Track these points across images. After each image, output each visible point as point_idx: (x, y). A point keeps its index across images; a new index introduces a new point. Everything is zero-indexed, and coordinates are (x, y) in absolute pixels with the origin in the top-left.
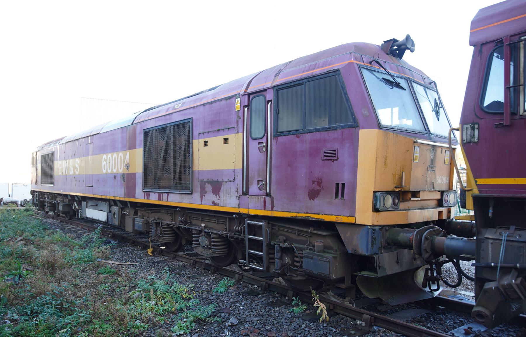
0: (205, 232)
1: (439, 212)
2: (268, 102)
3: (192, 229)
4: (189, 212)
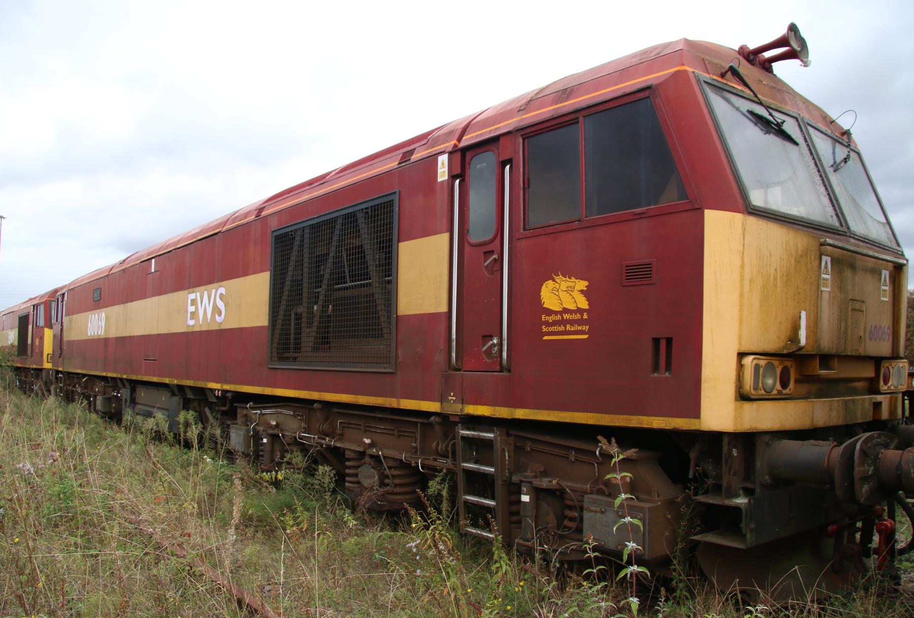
0: (372, 456)
3: (344, 450)
4: (338, 412)
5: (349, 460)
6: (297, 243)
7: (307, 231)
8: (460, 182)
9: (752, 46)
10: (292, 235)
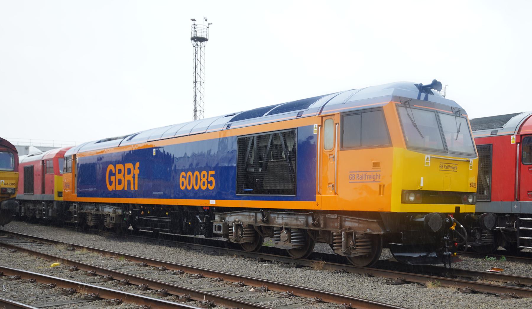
0: (286, 229)
1: (456, 207)
2: (336, 124)
3: (273, 227)
5: (275, 231)
6: (250, 143)
7: (255, 138)
8: (320, 128)
9: (424, 84)
10: (246, 139)
